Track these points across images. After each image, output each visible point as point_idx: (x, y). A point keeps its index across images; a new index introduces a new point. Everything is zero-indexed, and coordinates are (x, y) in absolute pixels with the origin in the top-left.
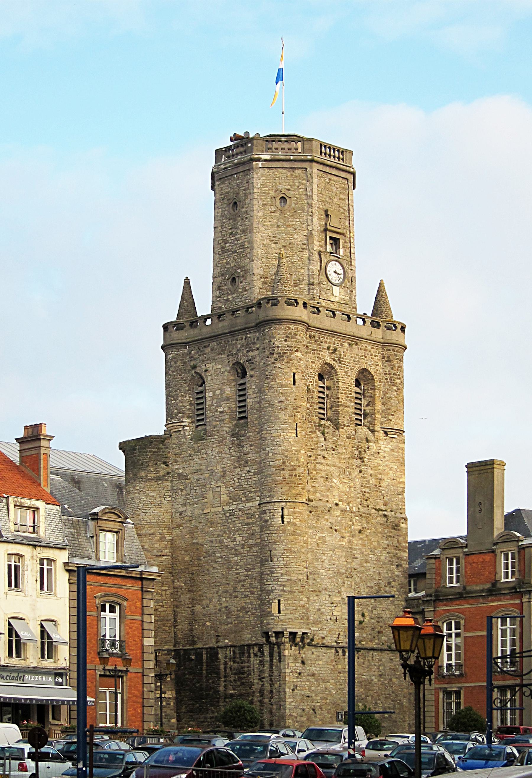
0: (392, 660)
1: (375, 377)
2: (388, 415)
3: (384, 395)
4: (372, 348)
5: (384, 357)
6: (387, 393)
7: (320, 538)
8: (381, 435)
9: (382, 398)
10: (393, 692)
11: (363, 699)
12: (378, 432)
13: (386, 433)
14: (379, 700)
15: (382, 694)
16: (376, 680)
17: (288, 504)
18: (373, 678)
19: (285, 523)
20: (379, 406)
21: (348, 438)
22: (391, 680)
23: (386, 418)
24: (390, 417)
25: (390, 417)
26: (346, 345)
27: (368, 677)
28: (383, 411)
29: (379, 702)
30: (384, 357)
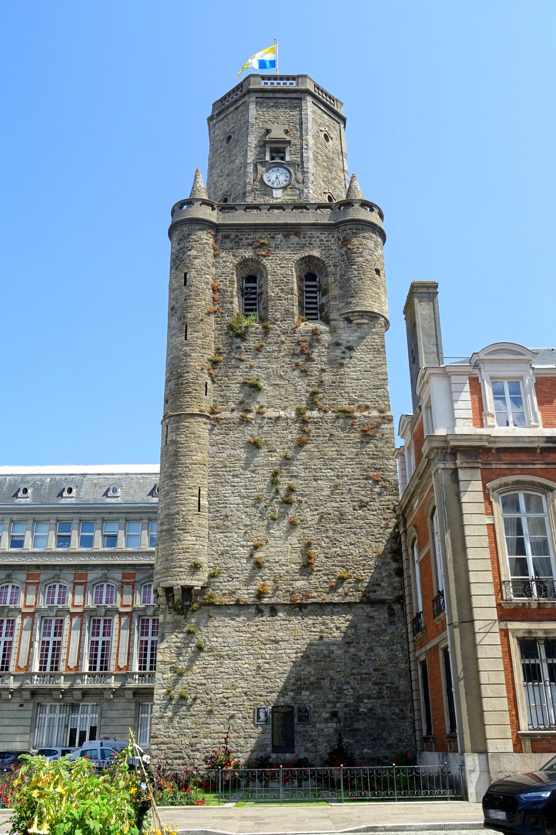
0: (372, 617)
1: (326, 262)
2: (347, 297)
3: (341, 278)
4: (321, 234)
5: (339, 240)
6: (344, 275)
7: (229, 456)
8: (342, 324)
9: (340, 282)
10: (375, 670)
11: (312, 684)
12: (335, 320)
13: (349, 321)
14: (348, 683)
15: (352, 674)
16: (340, 652)
17: (172, 418)
18: (334, 648)
19: (168, 443)
20: (335, 291)
21: (284, 333)
22: (371, 649)
23: (343, 302)
24: (349, 300)
25: (349, 300)
26: (280, 236)
27: (324, 648)
28: (341, 296)
29: (345, 687)
30: (339, 240)
